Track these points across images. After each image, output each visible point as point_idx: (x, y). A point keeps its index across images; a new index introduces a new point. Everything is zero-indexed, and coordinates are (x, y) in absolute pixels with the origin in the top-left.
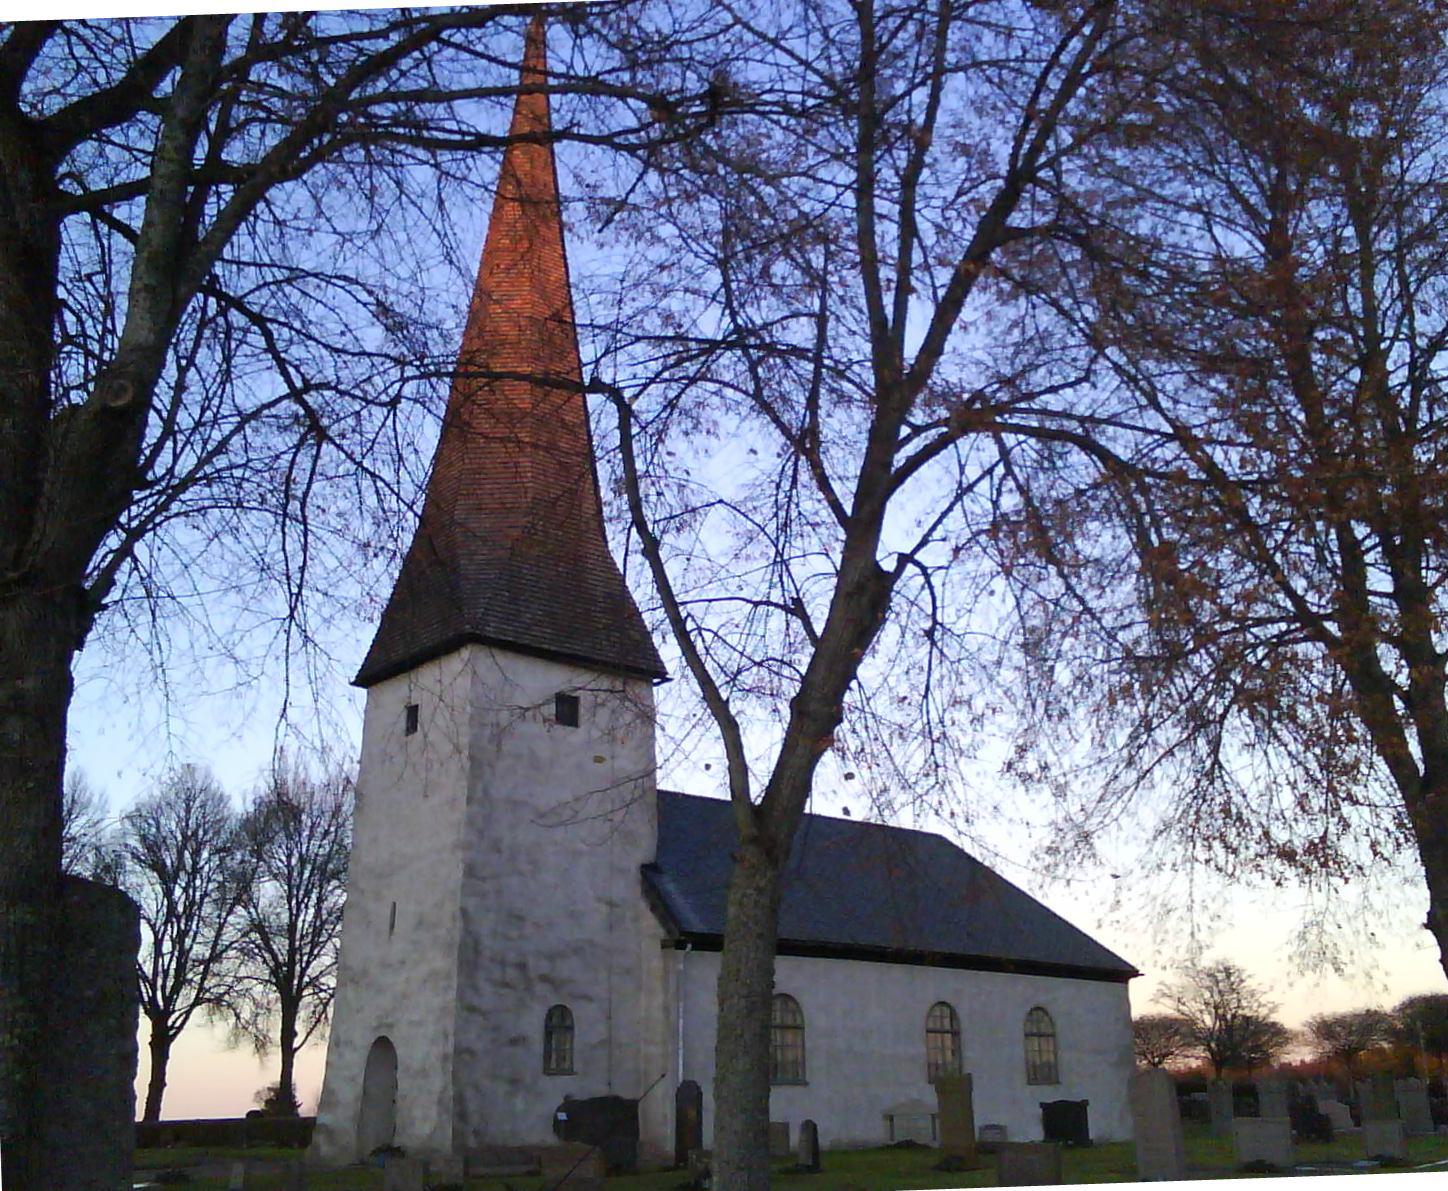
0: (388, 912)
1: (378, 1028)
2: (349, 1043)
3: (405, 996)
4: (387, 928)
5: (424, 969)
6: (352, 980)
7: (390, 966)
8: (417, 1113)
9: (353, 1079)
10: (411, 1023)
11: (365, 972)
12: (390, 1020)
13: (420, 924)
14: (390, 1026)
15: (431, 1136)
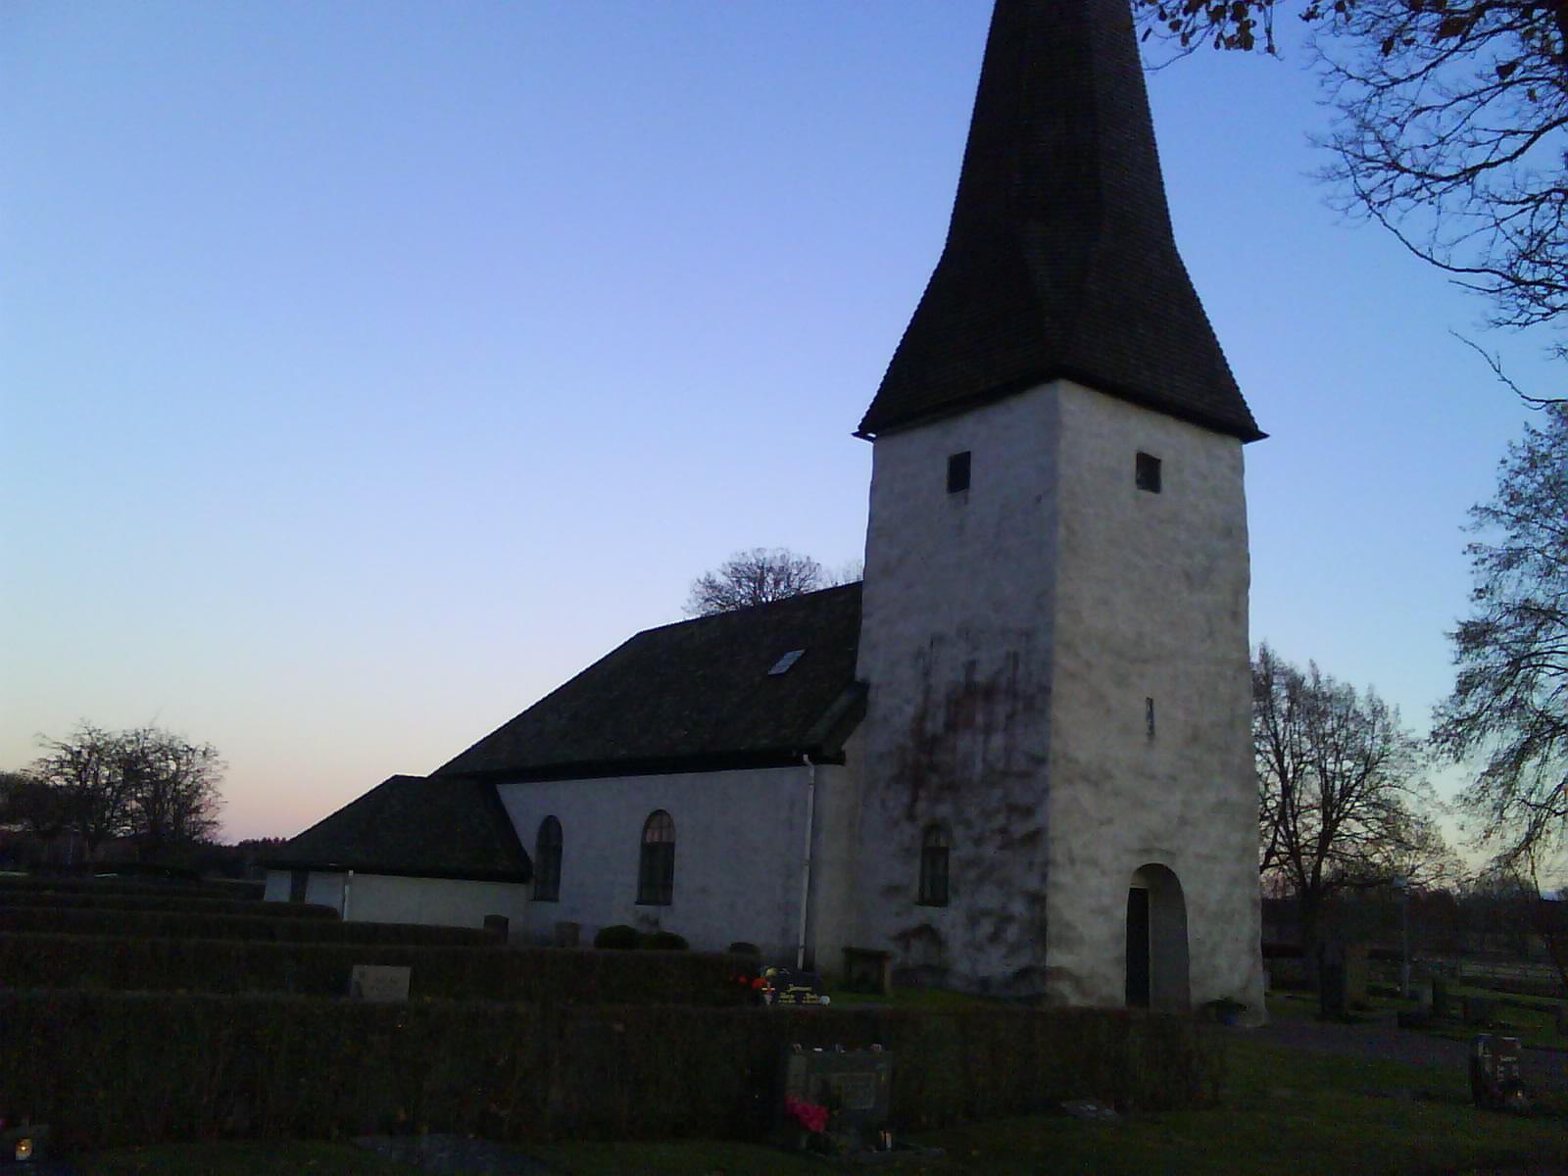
0: (1143, 707)
1: (1147, 851)
2: (1093, 862)
3: (1183, 821)
4: (1142, 724)
5: (1211, 797)
6: (1085, 778)
7: (1153, 777)
8: (1222, 962)
9: (1104, 912)
10: (1197, 856)
11: (1109, 776)
12: (1166, 846)
13: (1195, 738)
14: (1170, 854)
15: (1244, 989)
